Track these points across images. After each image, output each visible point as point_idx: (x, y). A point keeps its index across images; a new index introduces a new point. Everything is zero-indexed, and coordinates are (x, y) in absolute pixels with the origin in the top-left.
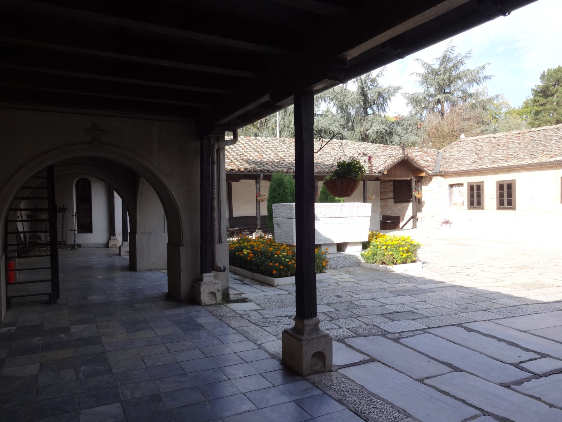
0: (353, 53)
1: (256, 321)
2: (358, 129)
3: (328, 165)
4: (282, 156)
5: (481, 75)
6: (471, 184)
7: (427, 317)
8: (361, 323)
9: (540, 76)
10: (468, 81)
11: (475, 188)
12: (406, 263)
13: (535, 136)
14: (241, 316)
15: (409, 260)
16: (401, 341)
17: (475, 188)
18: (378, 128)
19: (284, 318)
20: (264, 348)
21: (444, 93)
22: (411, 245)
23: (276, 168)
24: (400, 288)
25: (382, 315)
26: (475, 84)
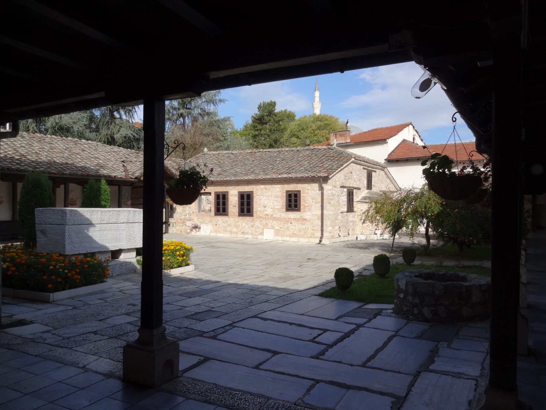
0: (214, 75)
1: (57, 343)
2: (104, 132)
3: (80, 167)
4: (22, 152)
5: (217, 98)
6: (218, 194)
7: (227, 313)
8: (172, 327)
9: (257, 106)
10: (206, 101)
11: (221, 197)
12: (181, 266)
13: (264, 156)
14: (33, 340)
15: (184, 264)
16: (219, 337)
17: (221, 197)
18: (127, 133)
19: (88, 335)
20: (92, 370)
21: (186, 108)
22: (186, 249)
23: (18, 166)
24: (186, 291)
25: (187, 317)
26: (212, 105)
